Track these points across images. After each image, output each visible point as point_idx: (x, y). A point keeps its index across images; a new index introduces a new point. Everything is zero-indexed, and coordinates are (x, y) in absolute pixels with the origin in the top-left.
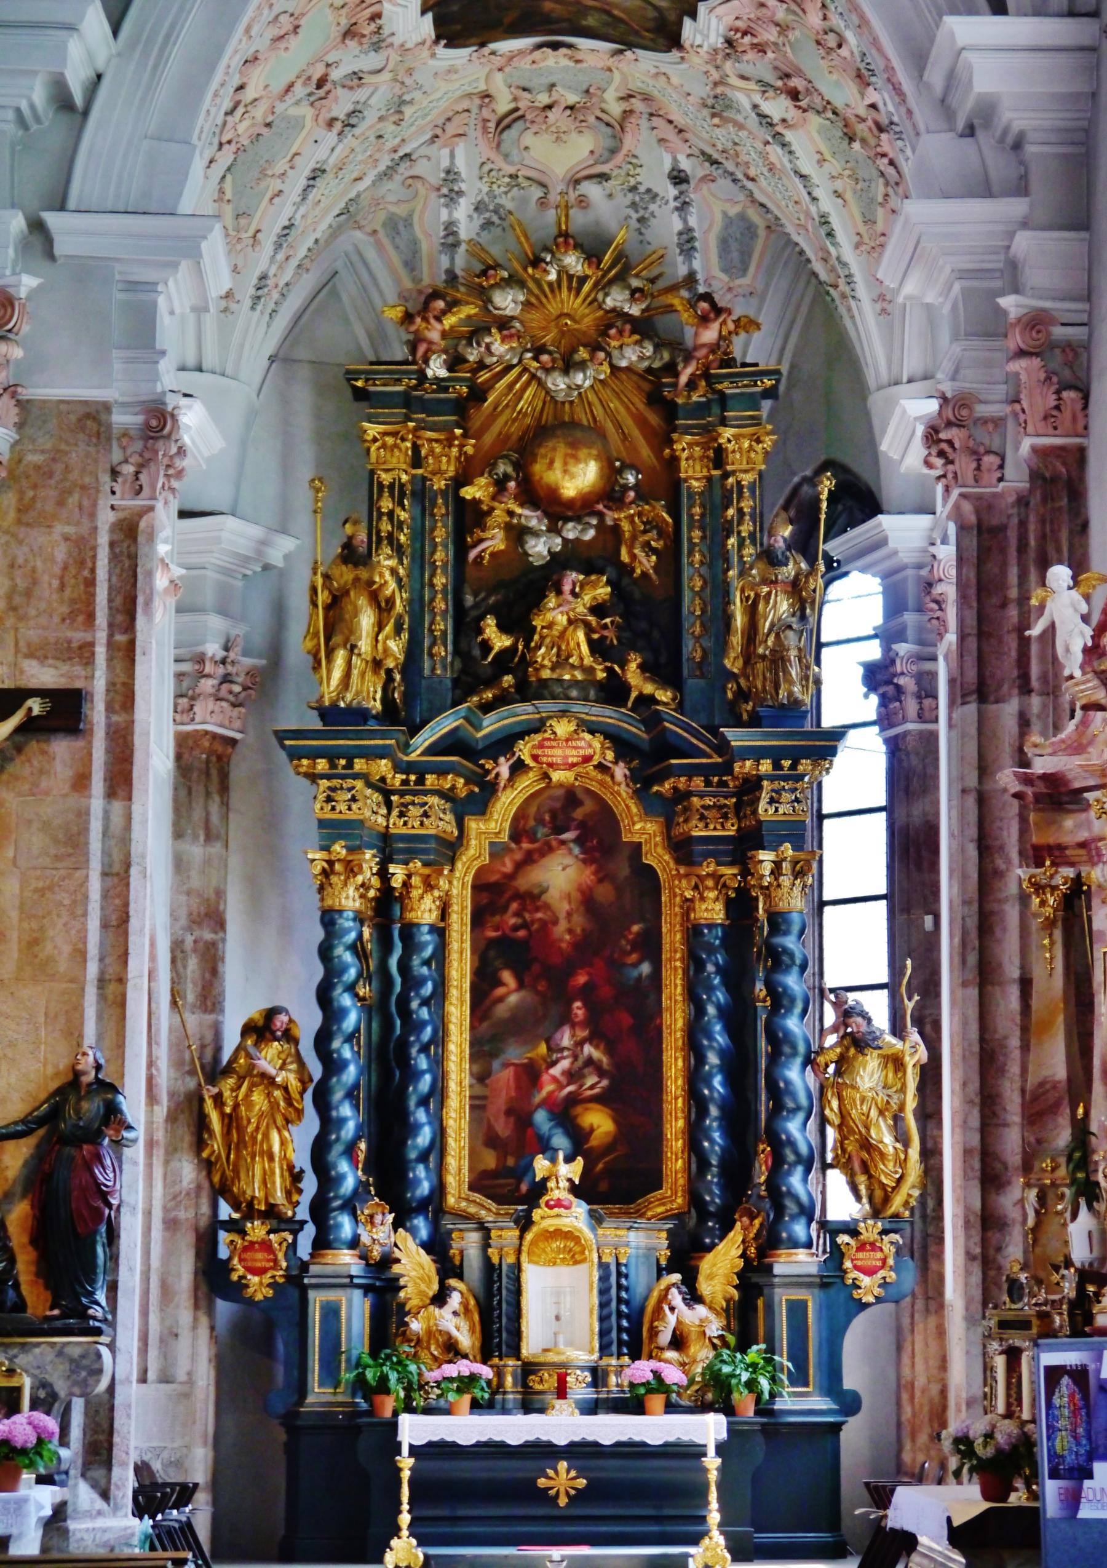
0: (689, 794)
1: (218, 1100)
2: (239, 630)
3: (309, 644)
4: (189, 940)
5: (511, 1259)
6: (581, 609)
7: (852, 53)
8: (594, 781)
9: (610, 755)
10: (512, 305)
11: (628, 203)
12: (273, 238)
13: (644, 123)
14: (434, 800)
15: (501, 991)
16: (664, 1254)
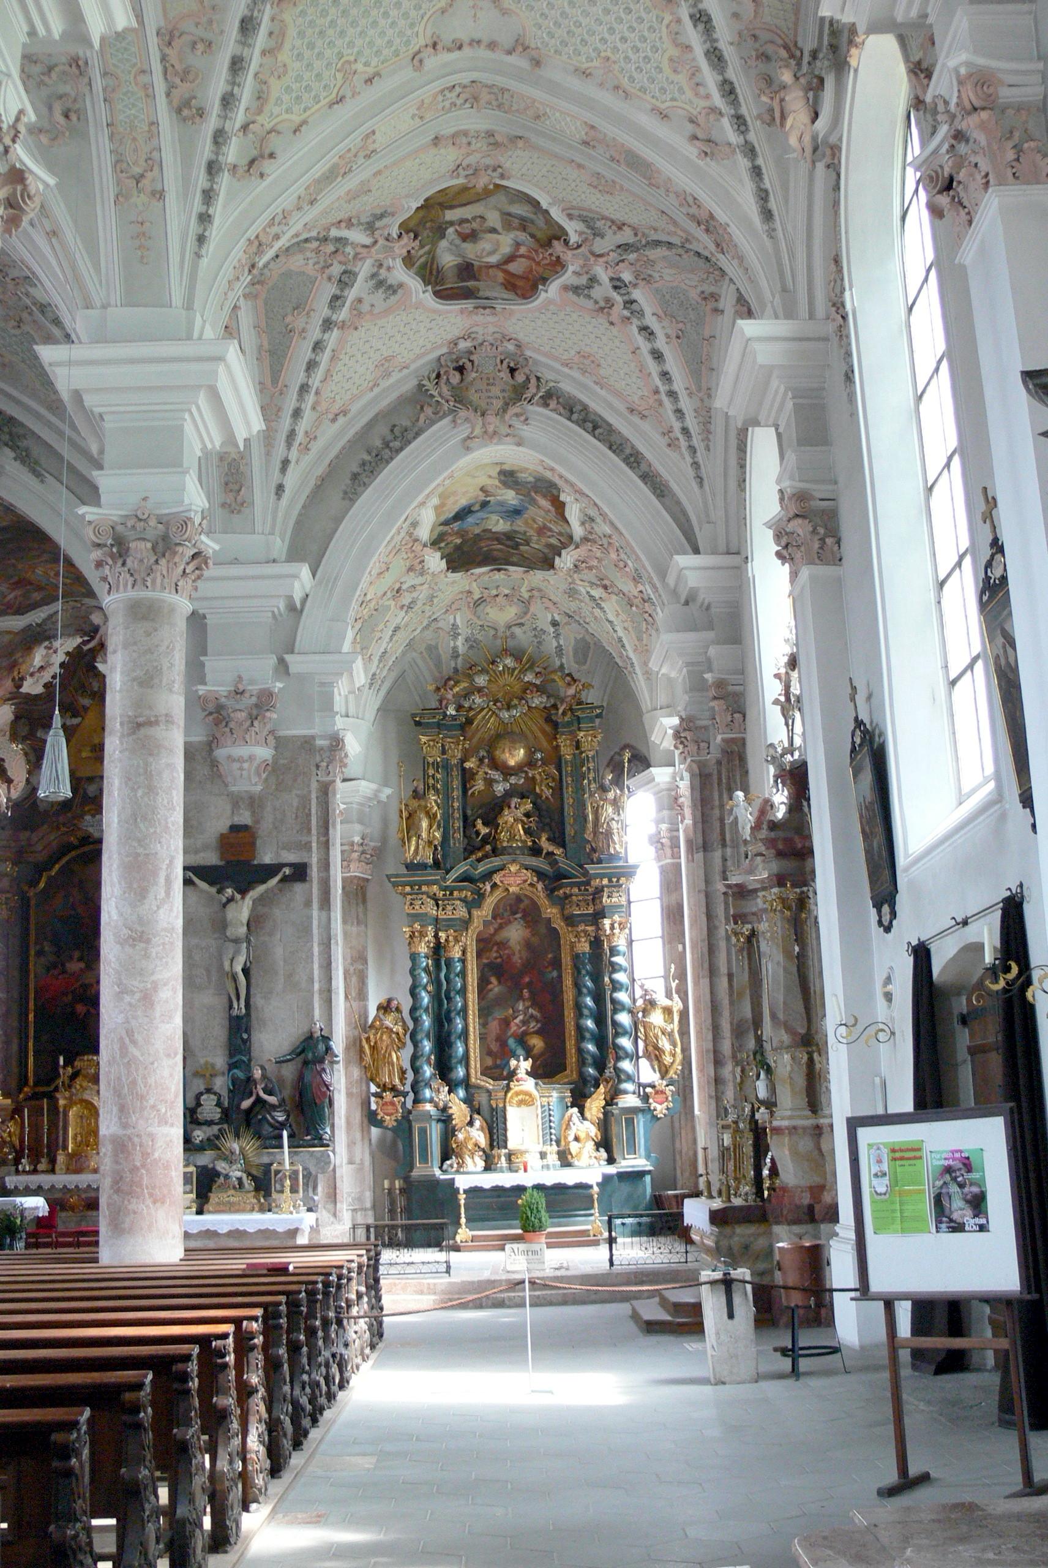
0: (571, 895)
1: (368, 1039)
2: (368, 831)
3: (400, 836)
4: (352, 969)
5: (501, 1105)
6: (519, 815)
8: (528, 891)
9: (535, 879)
13: (539, 601)
14: (458, 902)
15: (490, 986)
16: (569, 1100)
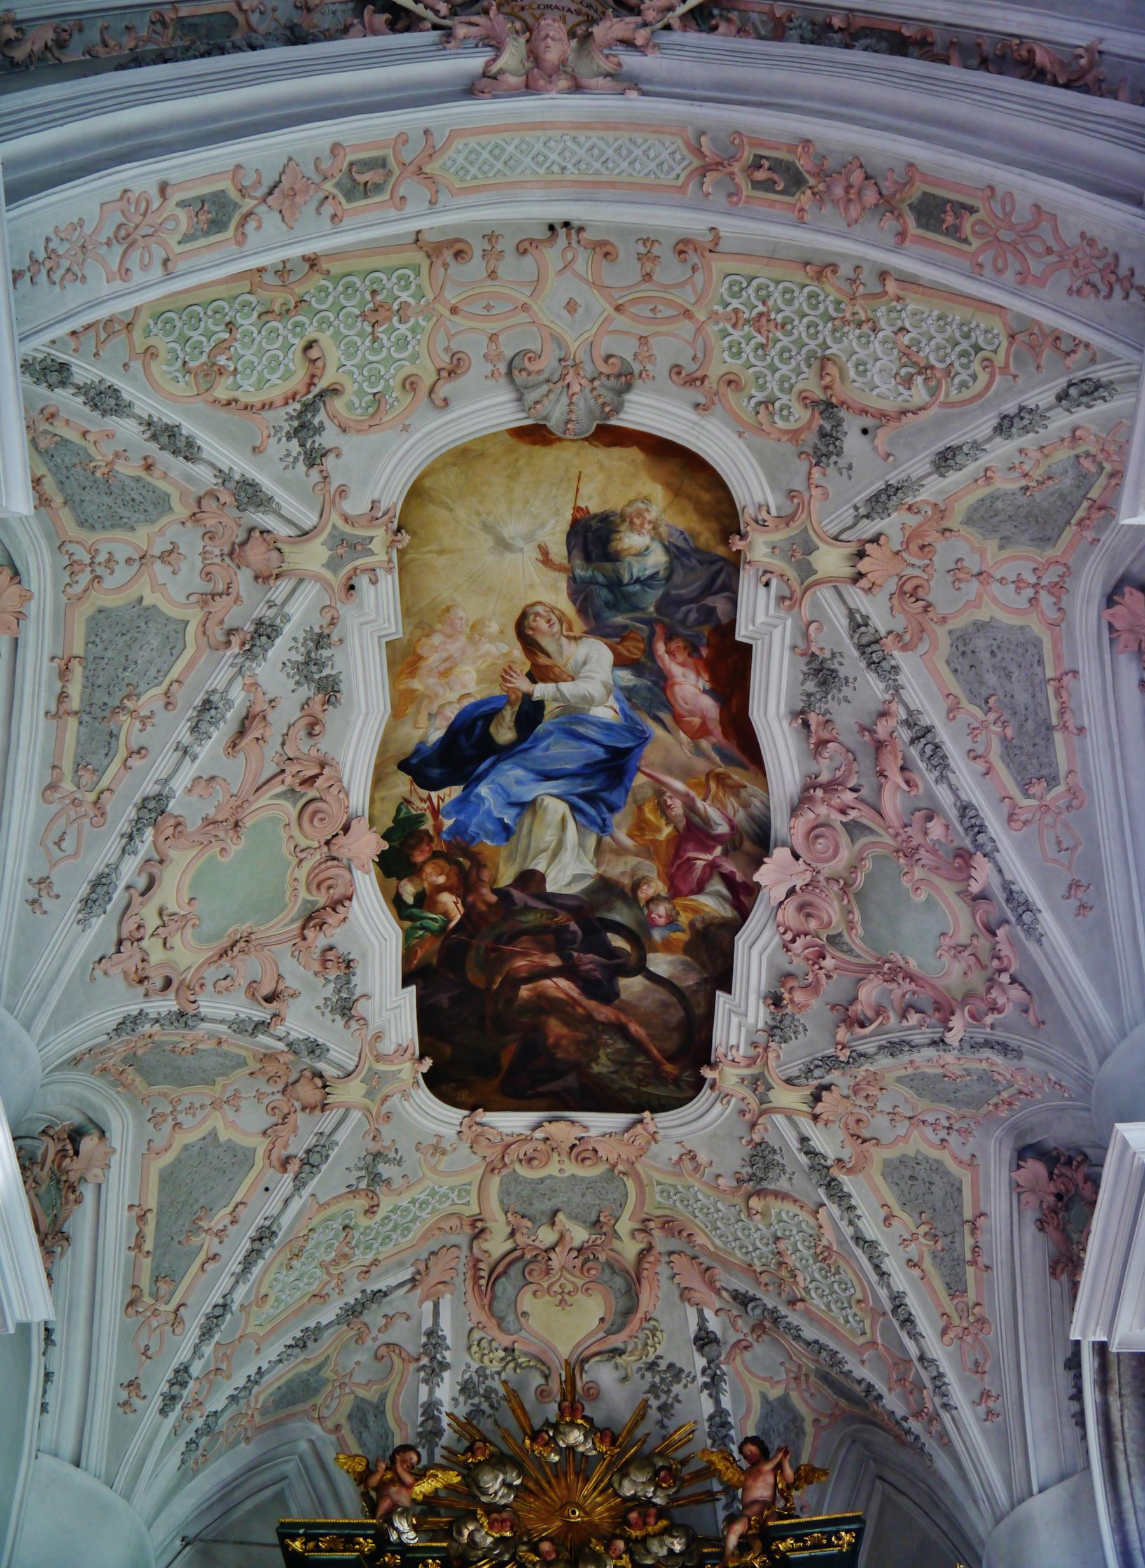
7: (947, 827)
10: (503, 1491)
11: (646, 1387)
12: (200, 1319)
13: (663, 1270)
